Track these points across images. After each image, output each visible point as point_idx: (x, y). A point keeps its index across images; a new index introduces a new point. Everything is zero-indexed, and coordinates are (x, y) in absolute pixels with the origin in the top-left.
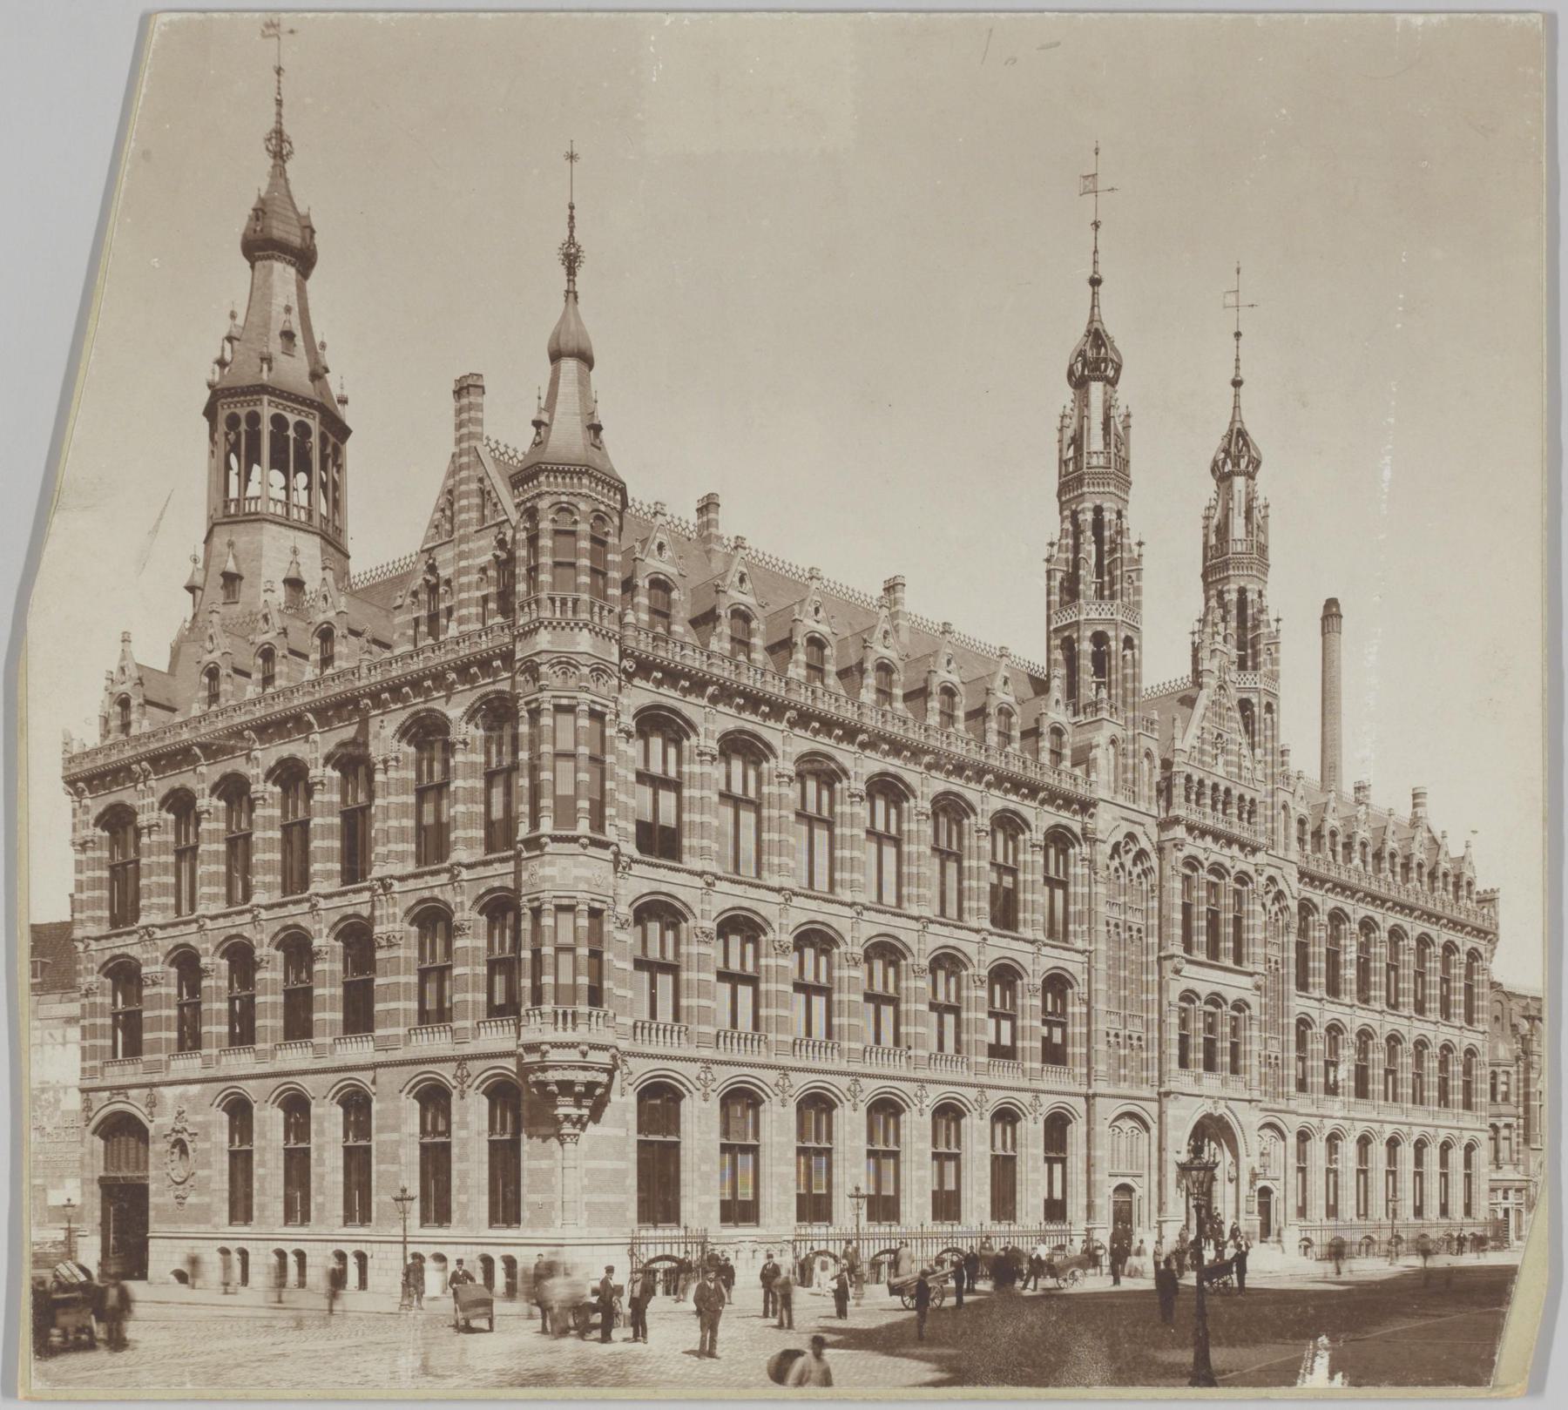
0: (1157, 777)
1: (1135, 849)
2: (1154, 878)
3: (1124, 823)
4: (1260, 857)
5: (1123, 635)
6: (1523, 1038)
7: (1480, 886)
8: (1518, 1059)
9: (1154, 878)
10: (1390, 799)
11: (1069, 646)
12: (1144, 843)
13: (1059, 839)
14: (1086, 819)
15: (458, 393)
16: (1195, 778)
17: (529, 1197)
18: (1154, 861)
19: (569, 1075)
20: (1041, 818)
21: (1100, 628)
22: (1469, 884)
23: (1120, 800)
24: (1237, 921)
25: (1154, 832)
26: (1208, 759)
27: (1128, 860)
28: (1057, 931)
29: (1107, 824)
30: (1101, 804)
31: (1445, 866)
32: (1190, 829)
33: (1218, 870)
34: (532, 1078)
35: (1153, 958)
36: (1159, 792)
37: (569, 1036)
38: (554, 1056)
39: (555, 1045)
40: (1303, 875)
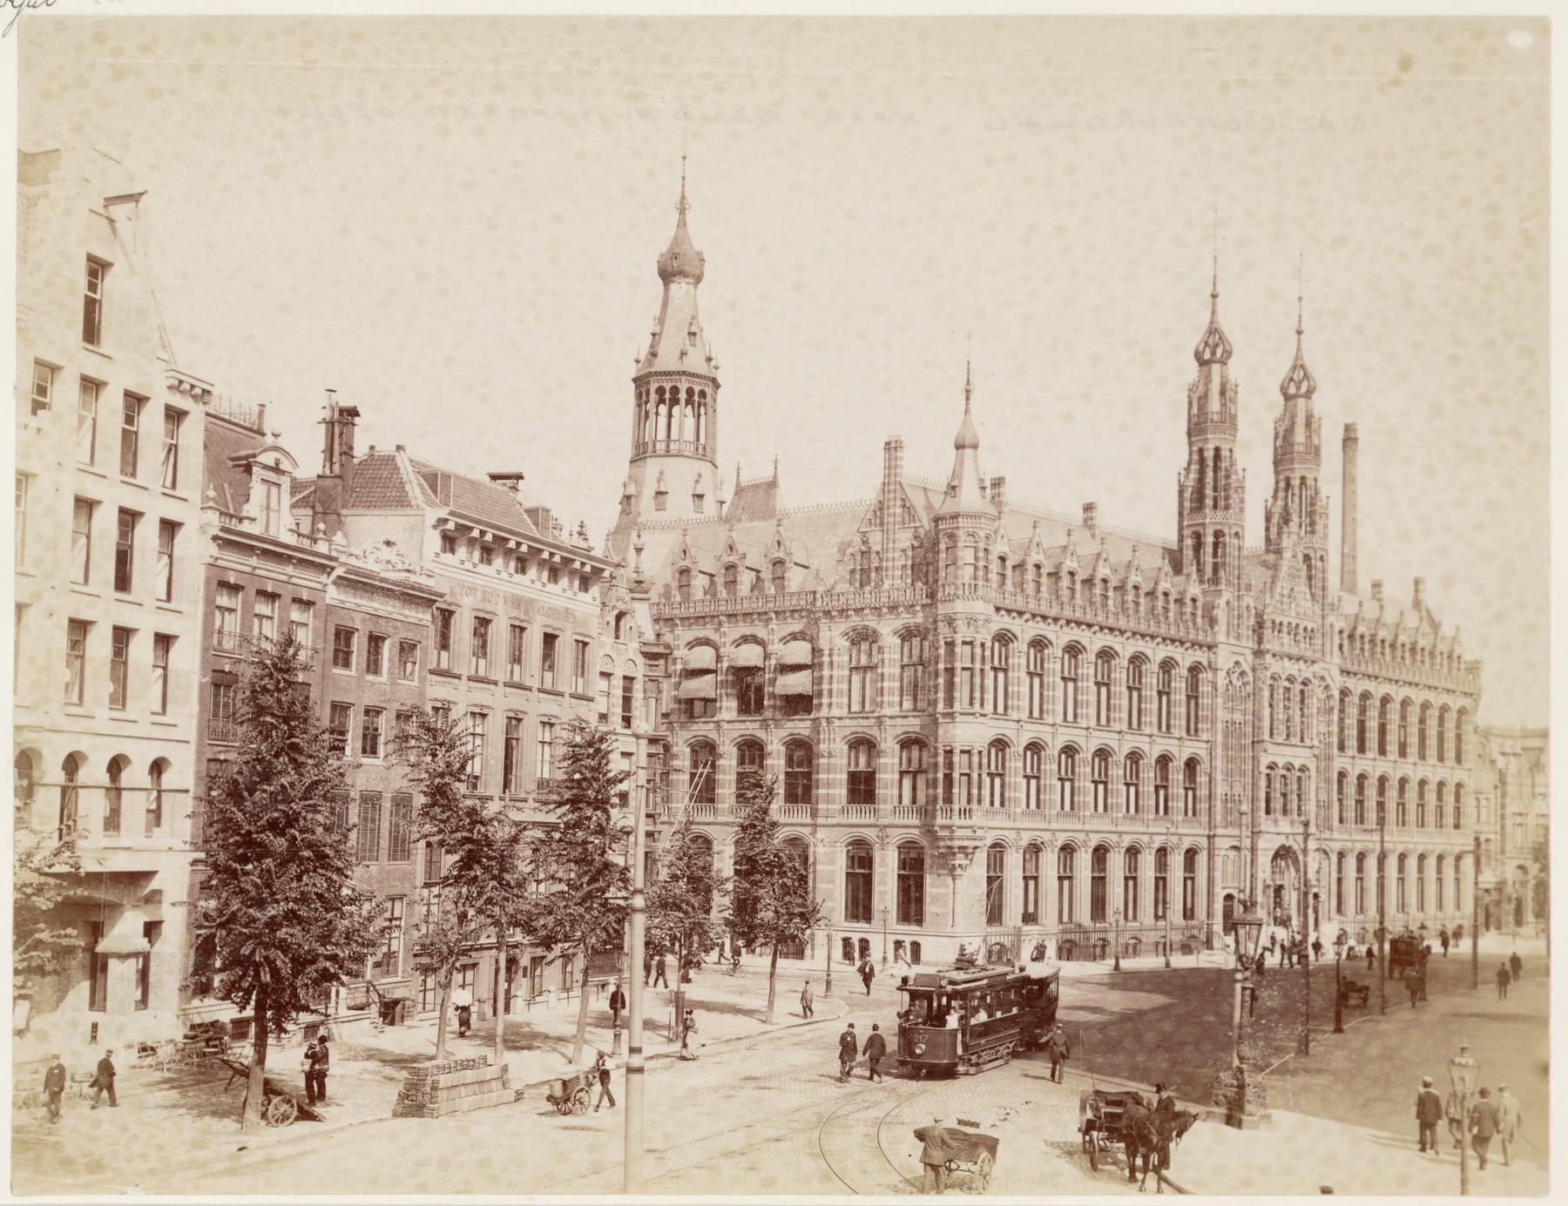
0: (1252, 621)
1: (1239, 671)
2: (1249, 689)
4: (1316, 667)
5: (1233, 532)
6: (1500, 771)
7: (1467, 657)
10: (1398, 593)
13: (1195, 670)
14: (1212, 655)
17: (930, 908)
19: (965, 843)
20: (1185, 658)
21: (1219, 527)
22: (1459, 657)
25: (1250, 658)
26: (1286, 607)
28: (1192, 730)
29: (1224, 659)
31: (1443, 647)
32: (1274, 655)
33: (1290, 679)
35: (1249, 741)
38: (959, 833)
39: (959, 827)
40: (1342, 671)
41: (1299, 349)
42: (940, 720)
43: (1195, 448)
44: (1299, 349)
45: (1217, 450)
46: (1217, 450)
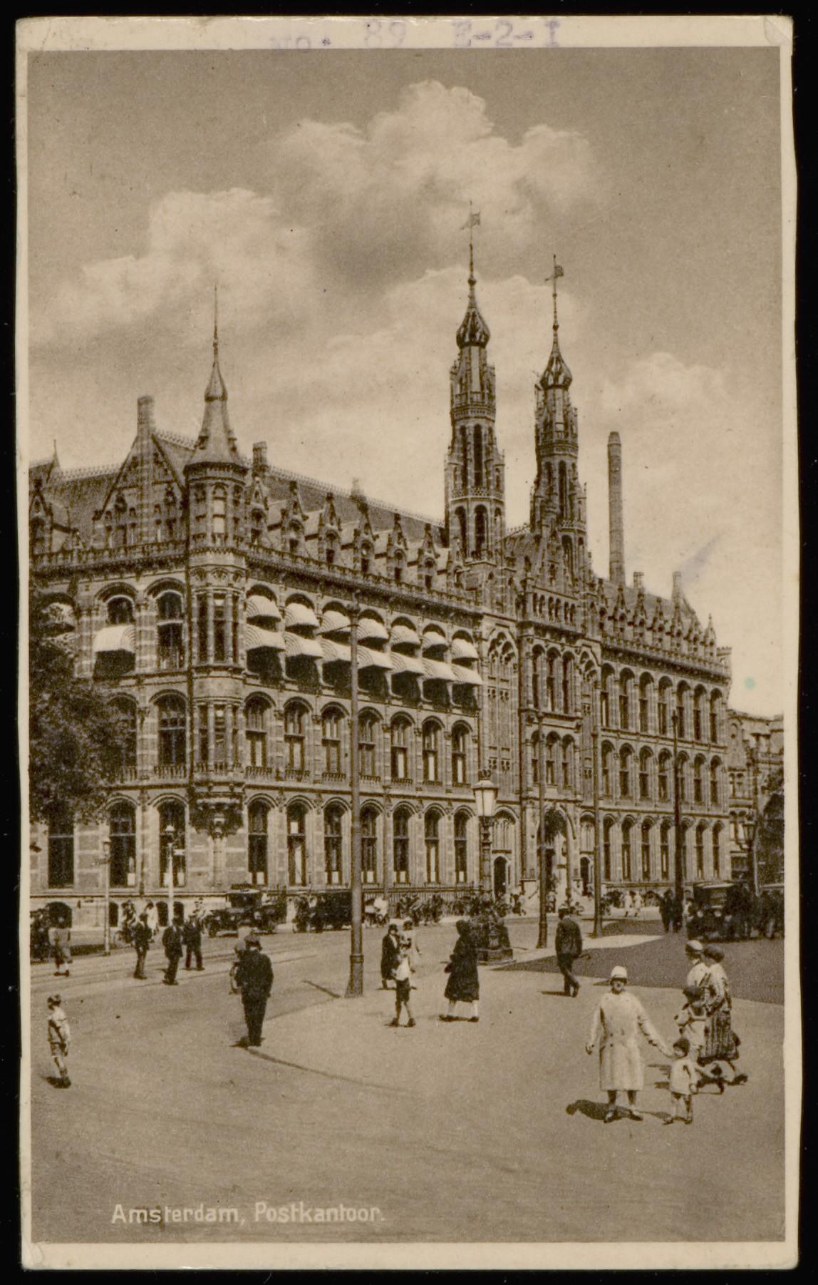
1: (503, 642)
2: (515, 660)
3: (497, 627)
8: (748, 765)
9: (515, 660)
10: (658, 586)
11: (461, 512)
12: (509, 638)
15: (140, 404)
16: (539, 596)
18: (515, 650)
23: (496, 612)
24: (565, 683)
25: (514, 629)
27: (499, 649)
30: (485, 617)
33: (553, 654)
34: (199, 801)
36: (518, 606)
37: (223, 778)
40: (605, 649)
41: (556, 342)
42: (195, 675)
43: (458, 427)
44: (556, 342)
45: (478, 428)
46: (478, 428)
